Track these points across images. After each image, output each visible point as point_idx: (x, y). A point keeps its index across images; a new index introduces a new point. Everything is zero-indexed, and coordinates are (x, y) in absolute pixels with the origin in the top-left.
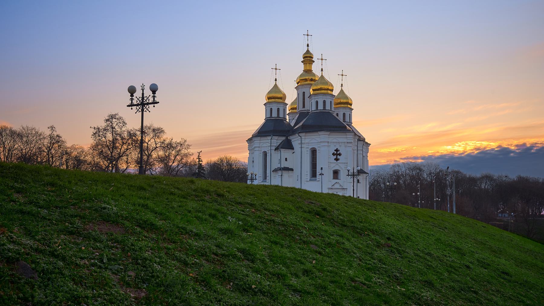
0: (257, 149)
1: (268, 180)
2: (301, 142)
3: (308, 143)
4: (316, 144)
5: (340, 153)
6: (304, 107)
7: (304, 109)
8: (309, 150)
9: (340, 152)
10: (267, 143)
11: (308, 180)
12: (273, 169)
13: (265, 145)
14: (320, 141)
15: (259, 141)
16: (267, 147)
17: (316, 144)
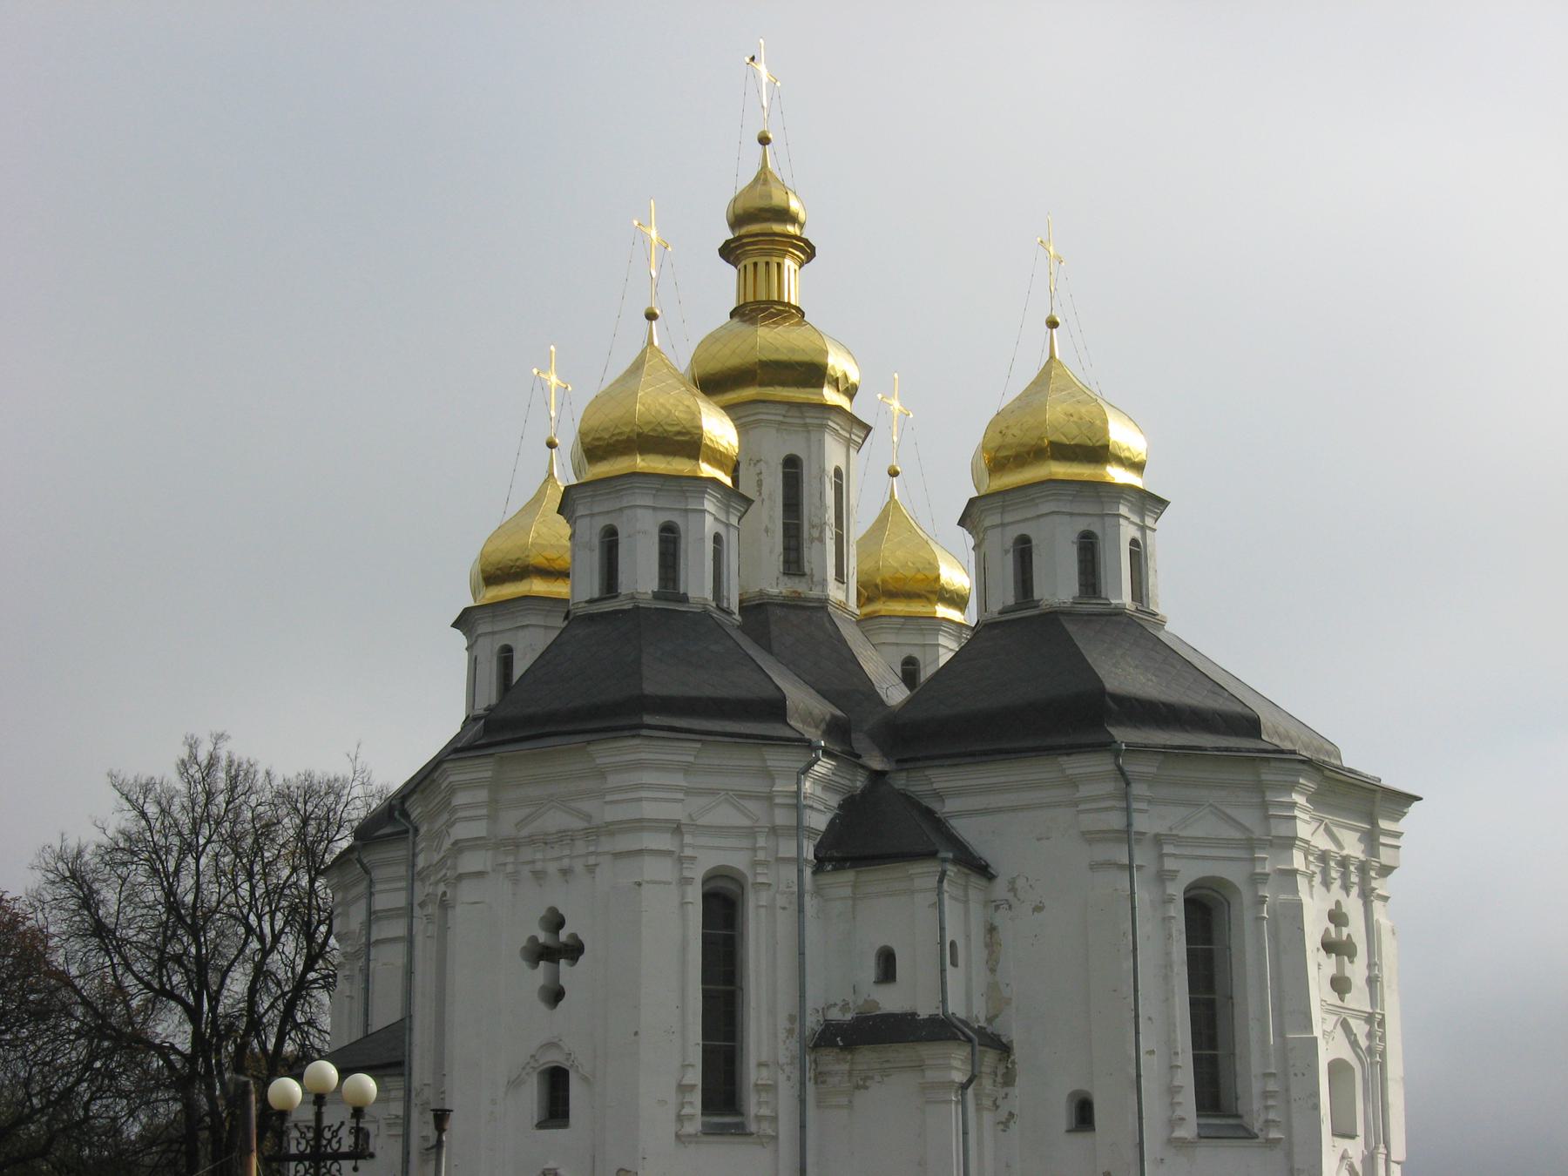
0: (664, 842)
1: (774, 1119)
2: (1129, 825)
3: (1177, 840)
4: (1233, 854)
5: (1349, 936)
6: (793, 563)
7: (800, 586)
8: (1177, 890)
9: (1355, 929)
10: (751, 805)
11: (1188, 1130)
12: (812, 1022)
13: (724, 815)
14: (1258, 833)
15: (679, 779)
16: (751, 832)
17: (1233, 854)
